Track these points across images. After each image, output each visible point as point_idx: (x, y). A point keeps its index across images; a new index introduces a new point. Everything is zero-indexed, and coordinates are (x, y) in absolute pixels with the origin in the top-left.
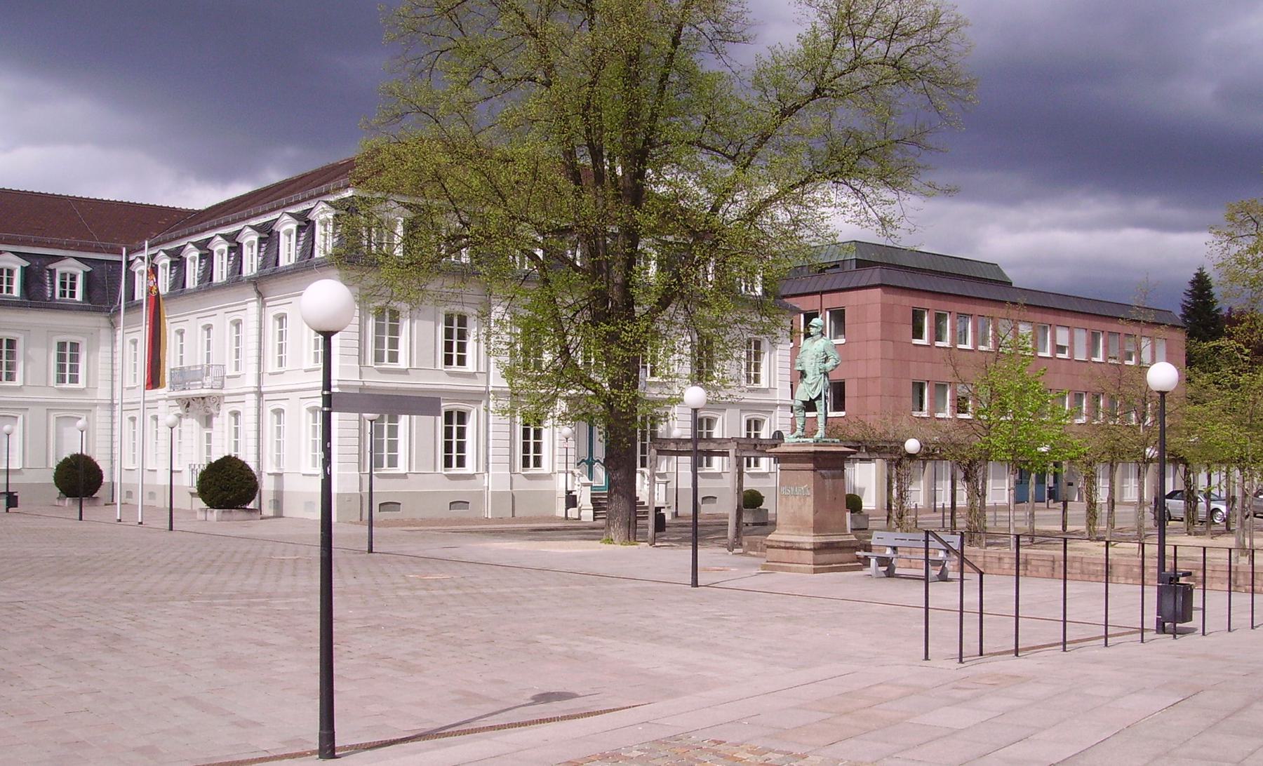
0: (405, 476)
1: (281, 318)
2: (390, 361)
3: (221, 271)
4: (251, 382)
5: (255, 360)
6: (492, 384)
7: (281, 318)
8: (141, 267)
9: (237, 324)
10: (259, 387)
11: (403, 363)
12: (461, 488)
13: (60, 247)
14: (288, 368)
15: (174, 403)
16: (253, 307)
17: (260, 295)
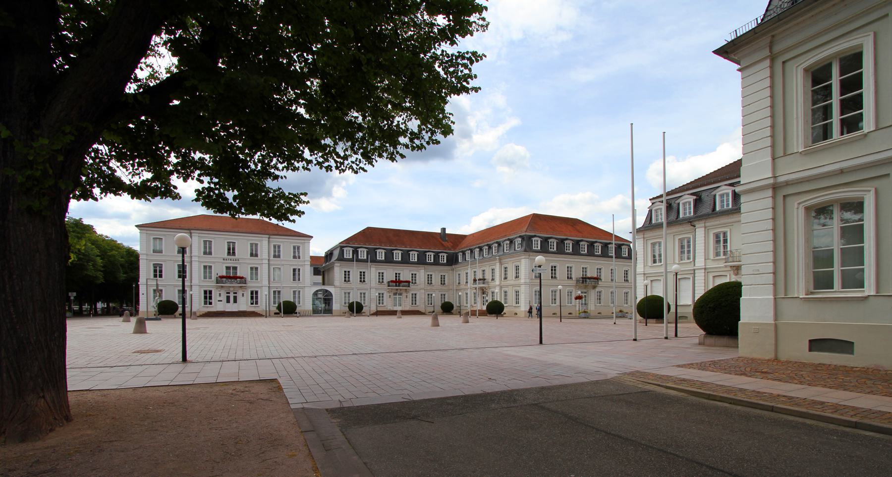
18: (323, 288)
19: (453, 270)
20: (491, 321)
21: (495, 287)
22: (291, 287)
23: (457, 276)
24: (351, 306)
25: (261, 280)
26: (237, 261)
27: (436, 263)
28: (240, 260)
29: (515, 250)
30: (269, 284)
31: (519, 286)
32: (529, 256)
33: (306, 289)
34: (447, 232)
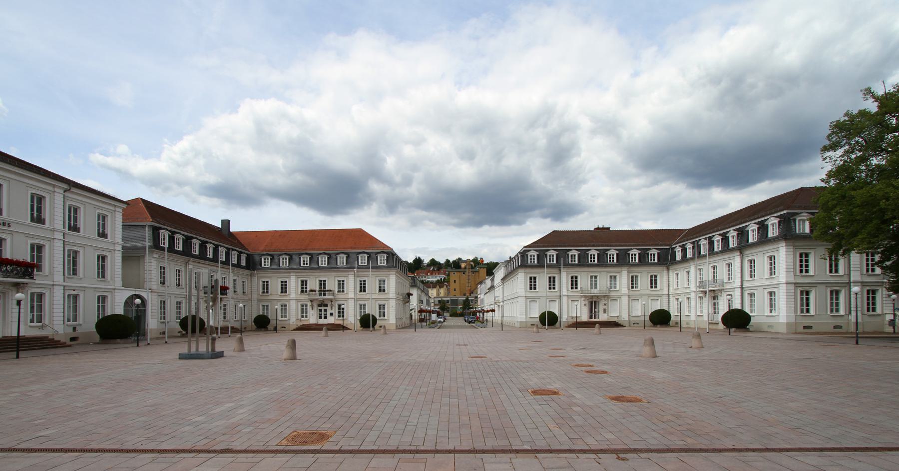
0: (813, 316)
1: (752, 262)
2: (806, 273)
3: (717, 247)
4: (739, 284)
5: (740, 276)
6: (852, 279)
7: (752, 262)
8: (678, 250)
9: (729, 265)
10: (742, 285)
11: (811, 272)
12: (838, 322)
13: (649, 246)
14: (756, 278)
15: (700, 293)
16: (737, 259)
17: (741, 253)
18: (137, 293)
19: (251, 275)
20: (368, 334)
21: (347, 299)
22: (96, 290)
23: (261, 284)
24: (183, 323)
25: (52, 273)
26: (6, 228)
27: (238, 265)
28: (12, 225)
29: (377, 264)
30: (64, 282)
31: (387, 299)
32: (396, 272)
33: (117, 293)
34: (233, 229)
